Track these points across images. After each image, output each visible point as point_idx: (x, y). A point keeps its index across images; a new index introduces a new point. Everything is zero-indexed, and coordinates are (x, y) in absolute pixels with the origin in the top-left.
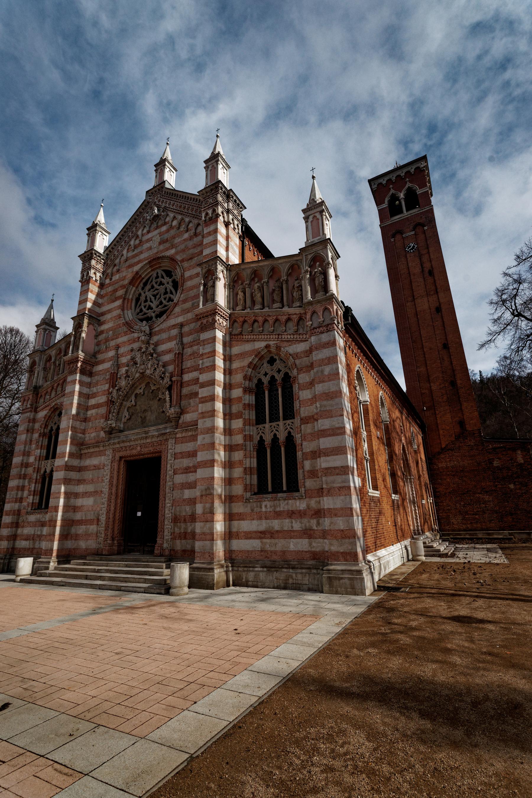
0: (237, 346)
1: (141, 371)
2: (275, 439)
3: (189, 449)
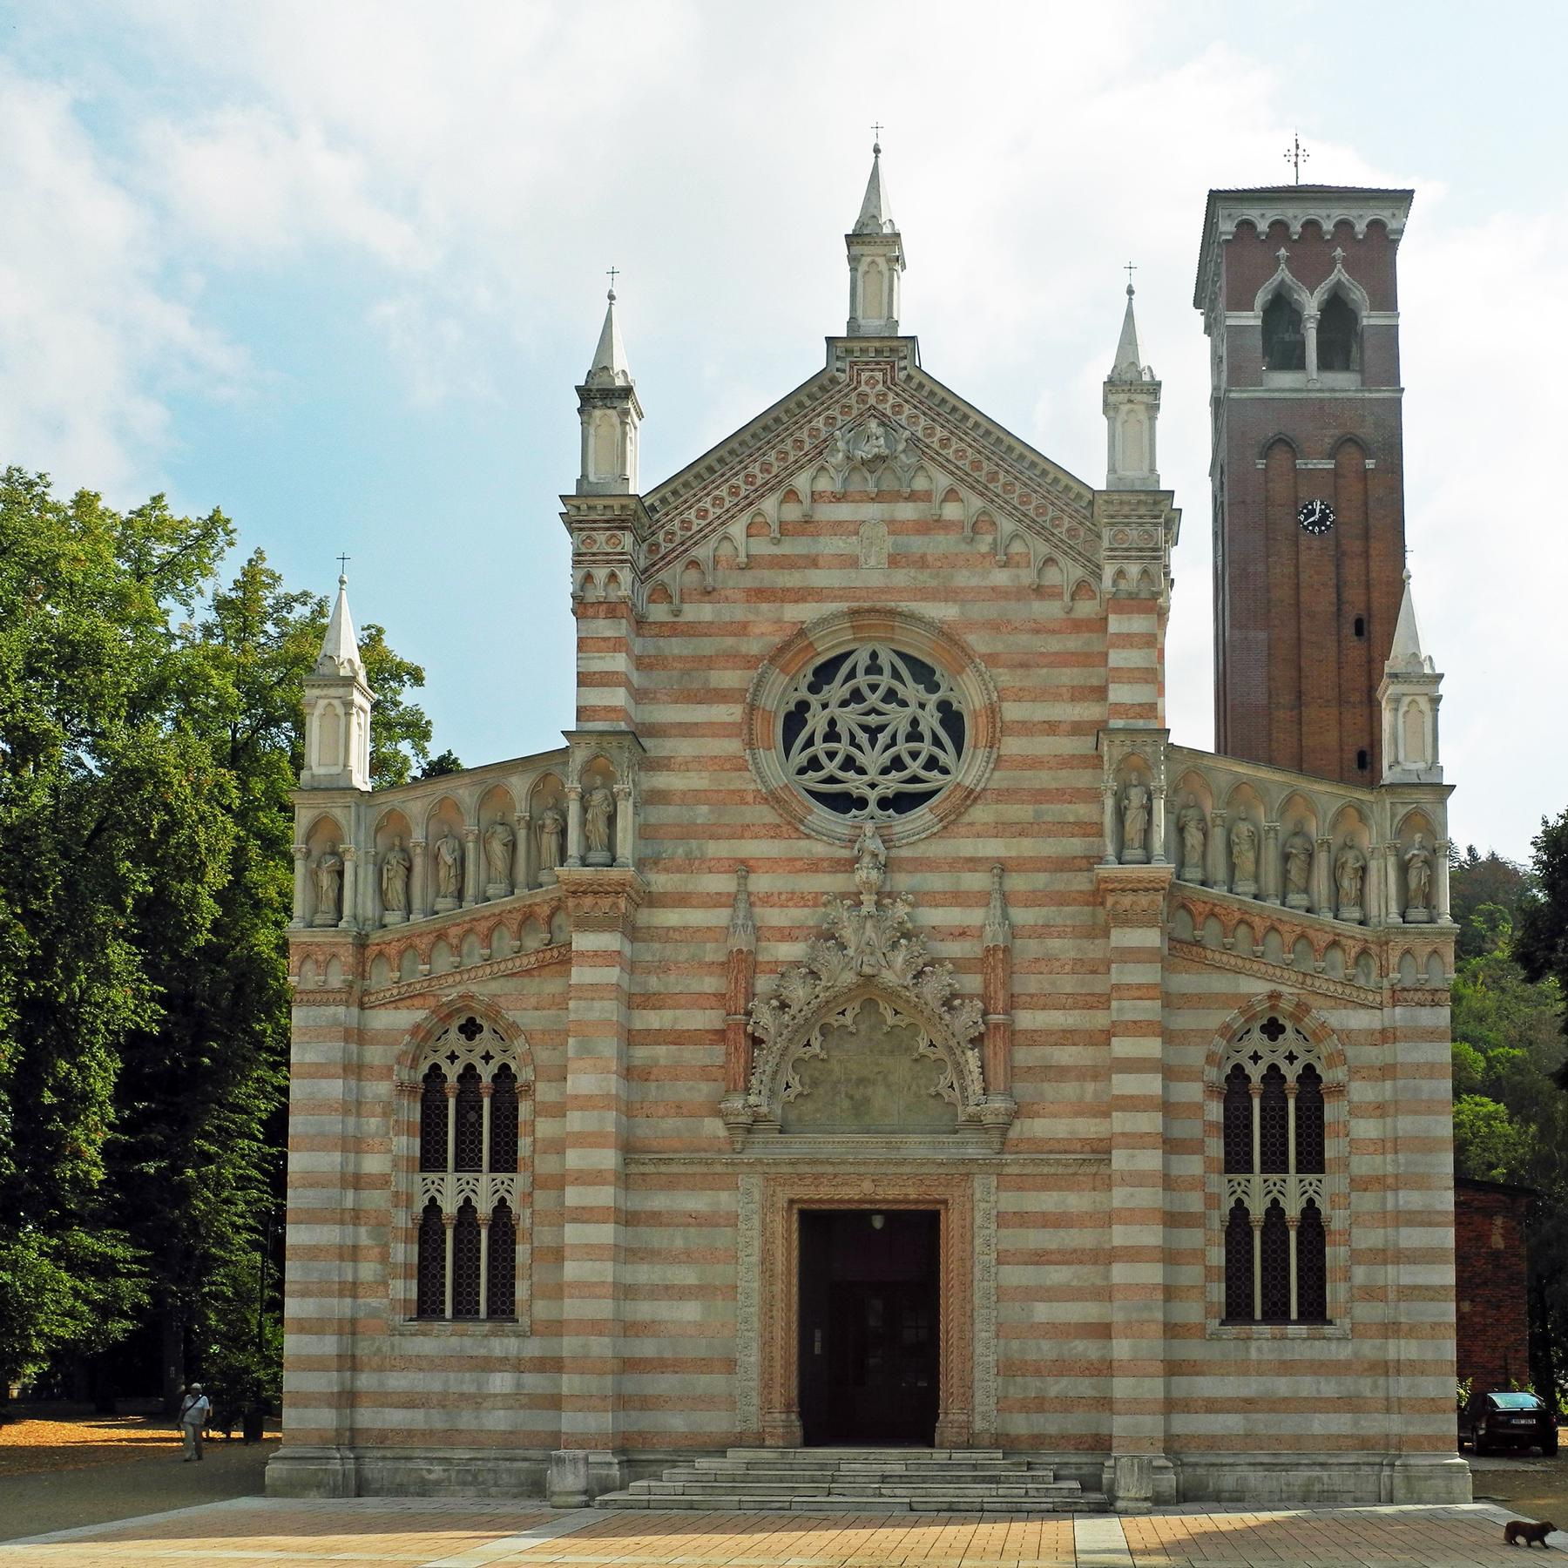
0: (1187, 972)
1: (867, 970)
2: (1275, 1211)
3: (1044, 1208)
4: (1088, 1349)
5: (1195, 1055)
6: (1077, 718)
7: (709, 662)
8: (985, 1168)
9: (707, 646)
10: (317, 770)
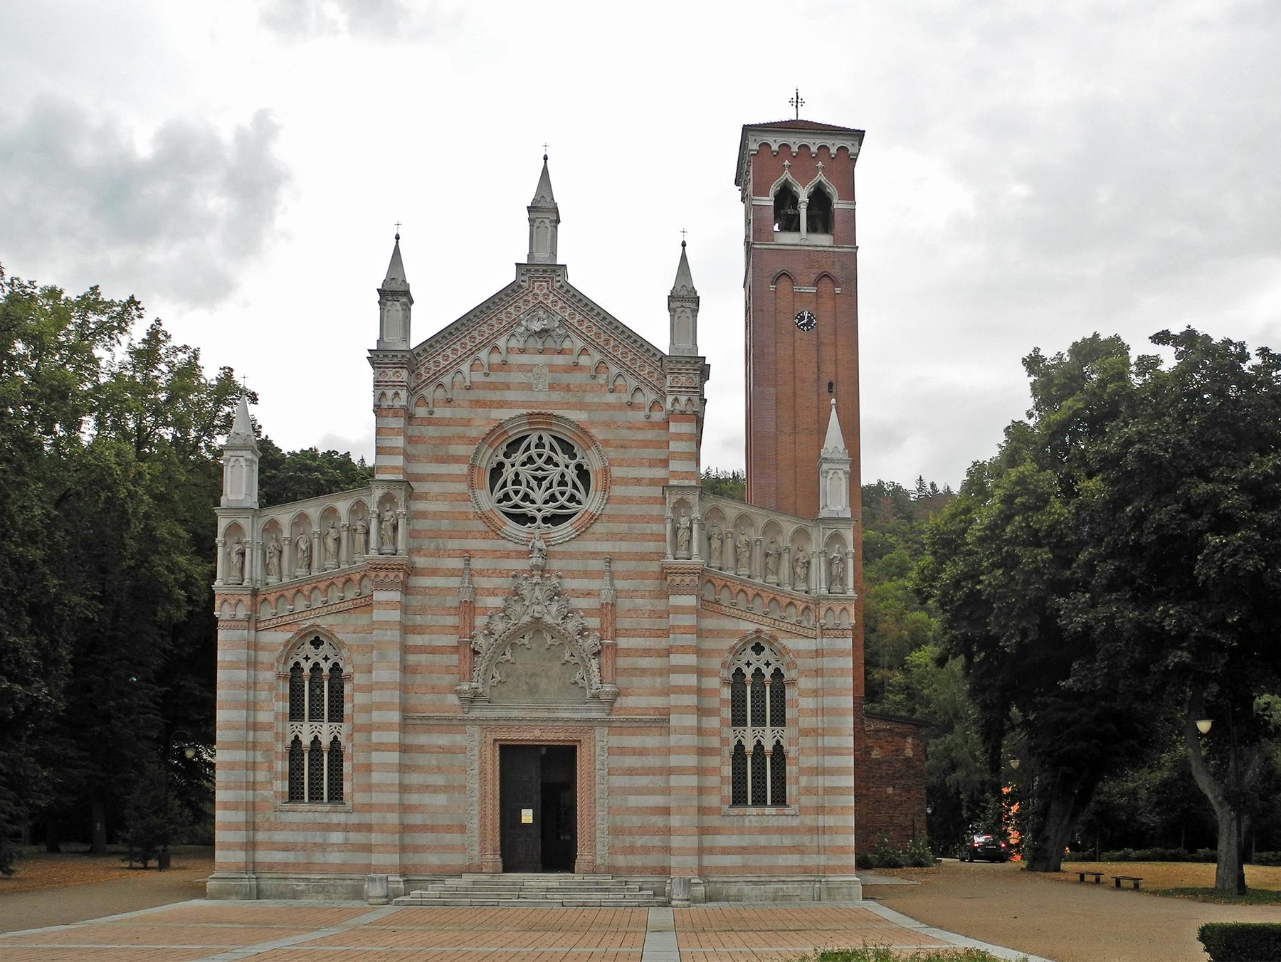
1: (536, 615)
2: (759, 746)
4: (658, 821)
5: (715, 663)
7: (447, 440)
9: (447, 431)
10: (231, 497)
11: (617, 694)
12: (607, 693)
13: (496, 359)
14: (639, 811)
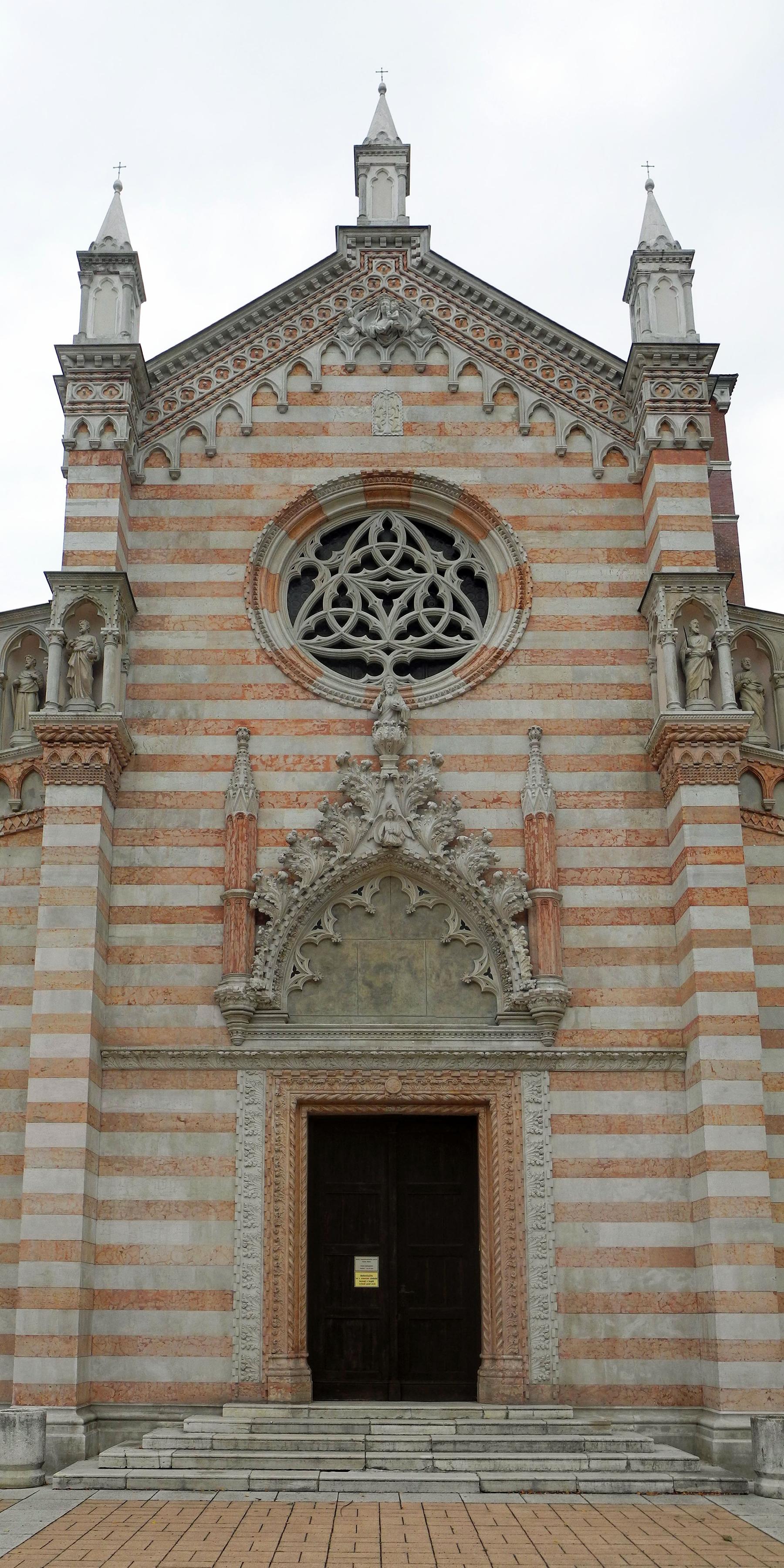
0: (757, 844)
1: (390, 839)
3: (607, 1111)
6: (616, 580)
7: (210, 523)
8: (535, 1064)
9: (206, 508)
11: (567, 1001)
12: (548, 998)
13: (301, 384)
14: (624, 1256)
